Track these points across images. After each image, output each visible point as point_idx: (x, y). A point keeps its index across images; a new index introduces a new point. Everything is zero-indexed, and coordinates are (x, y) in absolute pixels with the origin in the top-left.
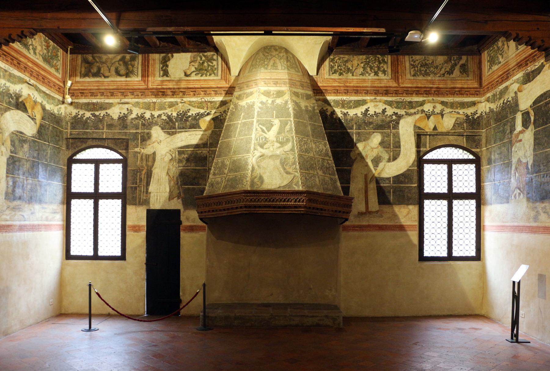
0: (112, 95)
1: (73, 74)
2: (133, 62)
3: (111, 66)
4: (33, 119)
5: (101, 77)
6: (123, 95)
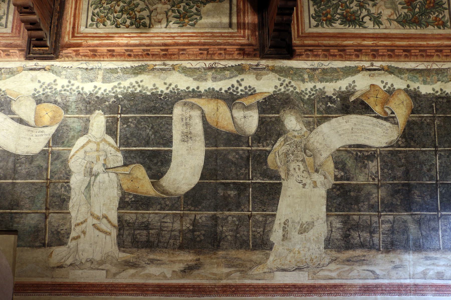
4: (390, 118)
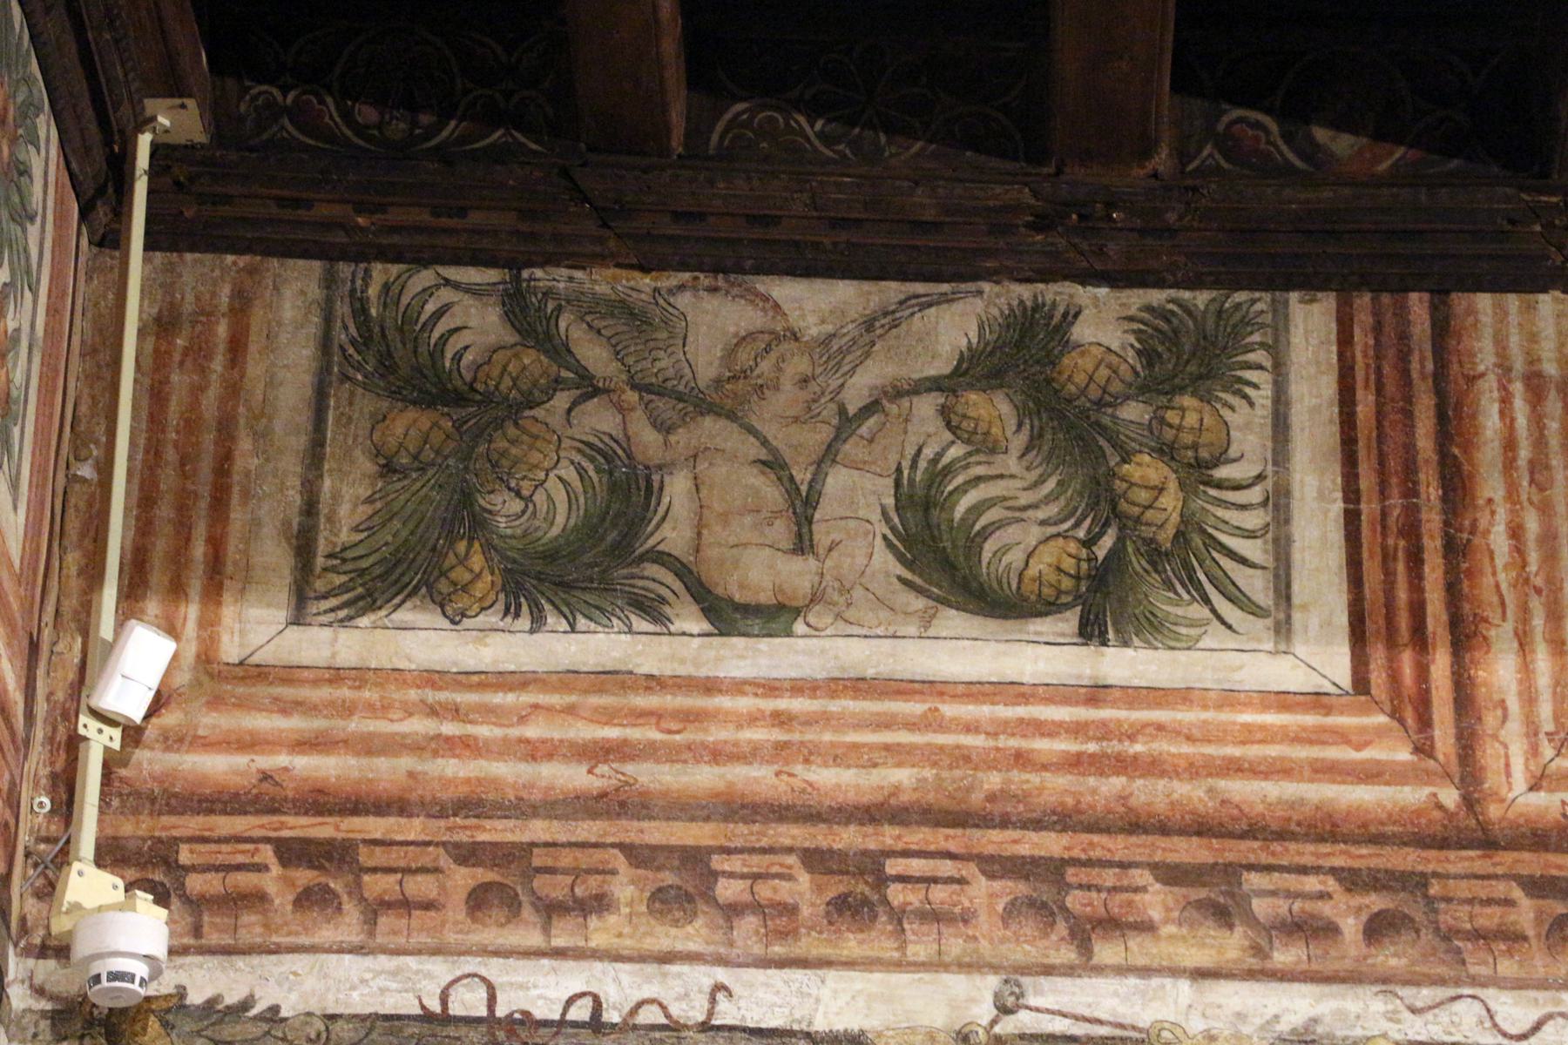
0: (851, 910)
1: (180, 558)
2: (1189, 412)
3: (829, 456)
5: (651, 608)
6: (1045, 912)
